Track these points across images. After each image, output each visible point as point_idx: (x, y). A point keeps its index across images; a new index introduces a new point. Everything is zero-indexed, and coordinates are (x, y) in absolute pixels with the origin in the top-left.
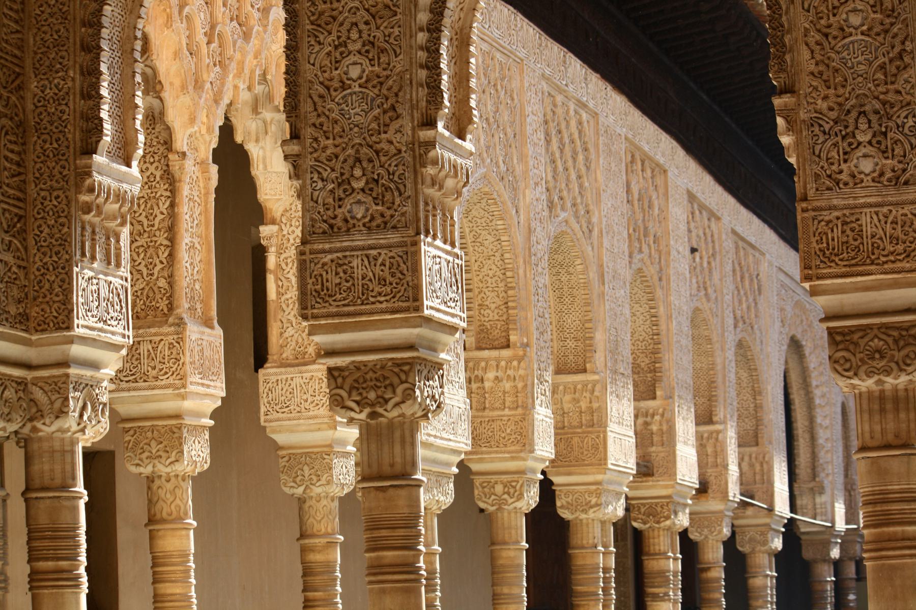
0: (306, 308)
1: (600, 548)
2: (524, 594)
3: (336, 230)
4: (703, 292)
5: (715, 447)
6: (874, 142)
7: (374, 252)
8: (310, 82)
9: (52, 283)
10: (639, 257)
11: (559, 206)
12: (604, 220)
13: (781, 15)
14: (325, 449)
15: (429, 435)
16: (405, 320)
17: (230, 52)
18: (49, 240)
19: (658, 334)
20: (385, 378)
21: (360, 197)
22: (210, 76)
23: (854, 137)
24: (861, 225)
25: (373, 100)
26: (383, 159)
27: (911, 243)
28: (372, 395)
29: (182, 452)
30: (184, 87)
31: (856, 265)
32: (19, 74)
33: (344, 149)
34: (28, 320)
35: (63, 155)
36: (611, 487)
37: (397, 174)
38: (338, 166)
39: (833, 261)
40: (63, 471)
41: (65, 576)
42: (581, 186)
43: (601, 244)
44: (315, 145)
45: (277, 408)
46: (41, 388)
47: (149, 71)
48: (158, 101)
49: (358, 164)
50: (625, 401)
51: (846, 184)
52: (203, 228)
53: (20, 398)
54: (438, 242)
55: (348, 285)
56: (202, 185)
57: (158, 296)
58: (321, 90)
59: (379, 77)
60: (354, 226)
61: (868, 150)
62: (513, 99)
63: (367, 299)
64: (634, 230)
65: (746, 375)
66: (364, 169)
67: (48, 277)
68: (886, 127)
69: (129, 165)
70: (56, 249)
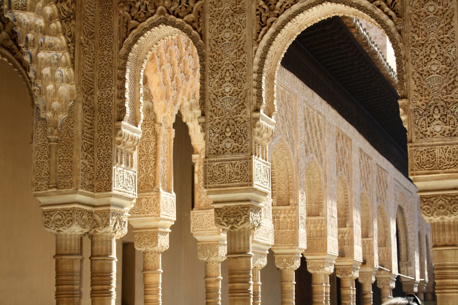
0: (206, 184)
1: (324, 285)
2: (294, 302)
3: (219, 153)
4: (365, 187)
5: (369, 246)
6: (441, 118)
7: (234, 162)
8: (210, 93)
9: (104, 173)
10: (341, 172)
11: (310, 152)
12: (327, 157)
13: (402, 67)
14: (216, 243)
15: (257, 238)
16: (246, 189)
17: (180, 85)
18: (103, 155)
19: (347, 202)
20: (238, 213)
21: (229, 139)
22: (172, 94)
23: (433, 116)
24: (435, 153)
25: (235, 101)
26: (238, 124)
27: (457, 160)
28: (232, 220)
29: (157, 242)
30: (161, 98)
32: (92, 88)
34: (94, 187)
35: (110, 121)
36: (328, 261)
37: (244, 131)
38: (221, 127)
40: (107, 249)
41: (106, 292)
42: (318, 144)
43: (326, 167)
44: (211, 119)
45: (197, 226)
46: (99, 215)
47: (147, 91)
48: (151, 103)
50: (334, 227)
51: (429, 136)
52: (168, 154)
53: (89, 219)
54: (260, 159)
55: (223, 175)
56: (168, 137)
57: (150, 180)
58: (214, 97)
59: (237, 91)
60: (226, 151)
61: (439, 122)
62: (292, 109)
64: (339, 162)
65: (381, 219)
66: (230, 129)
67: (102, 170)
68: (447, 113)
69: (137, 126)
70: (106, 159)
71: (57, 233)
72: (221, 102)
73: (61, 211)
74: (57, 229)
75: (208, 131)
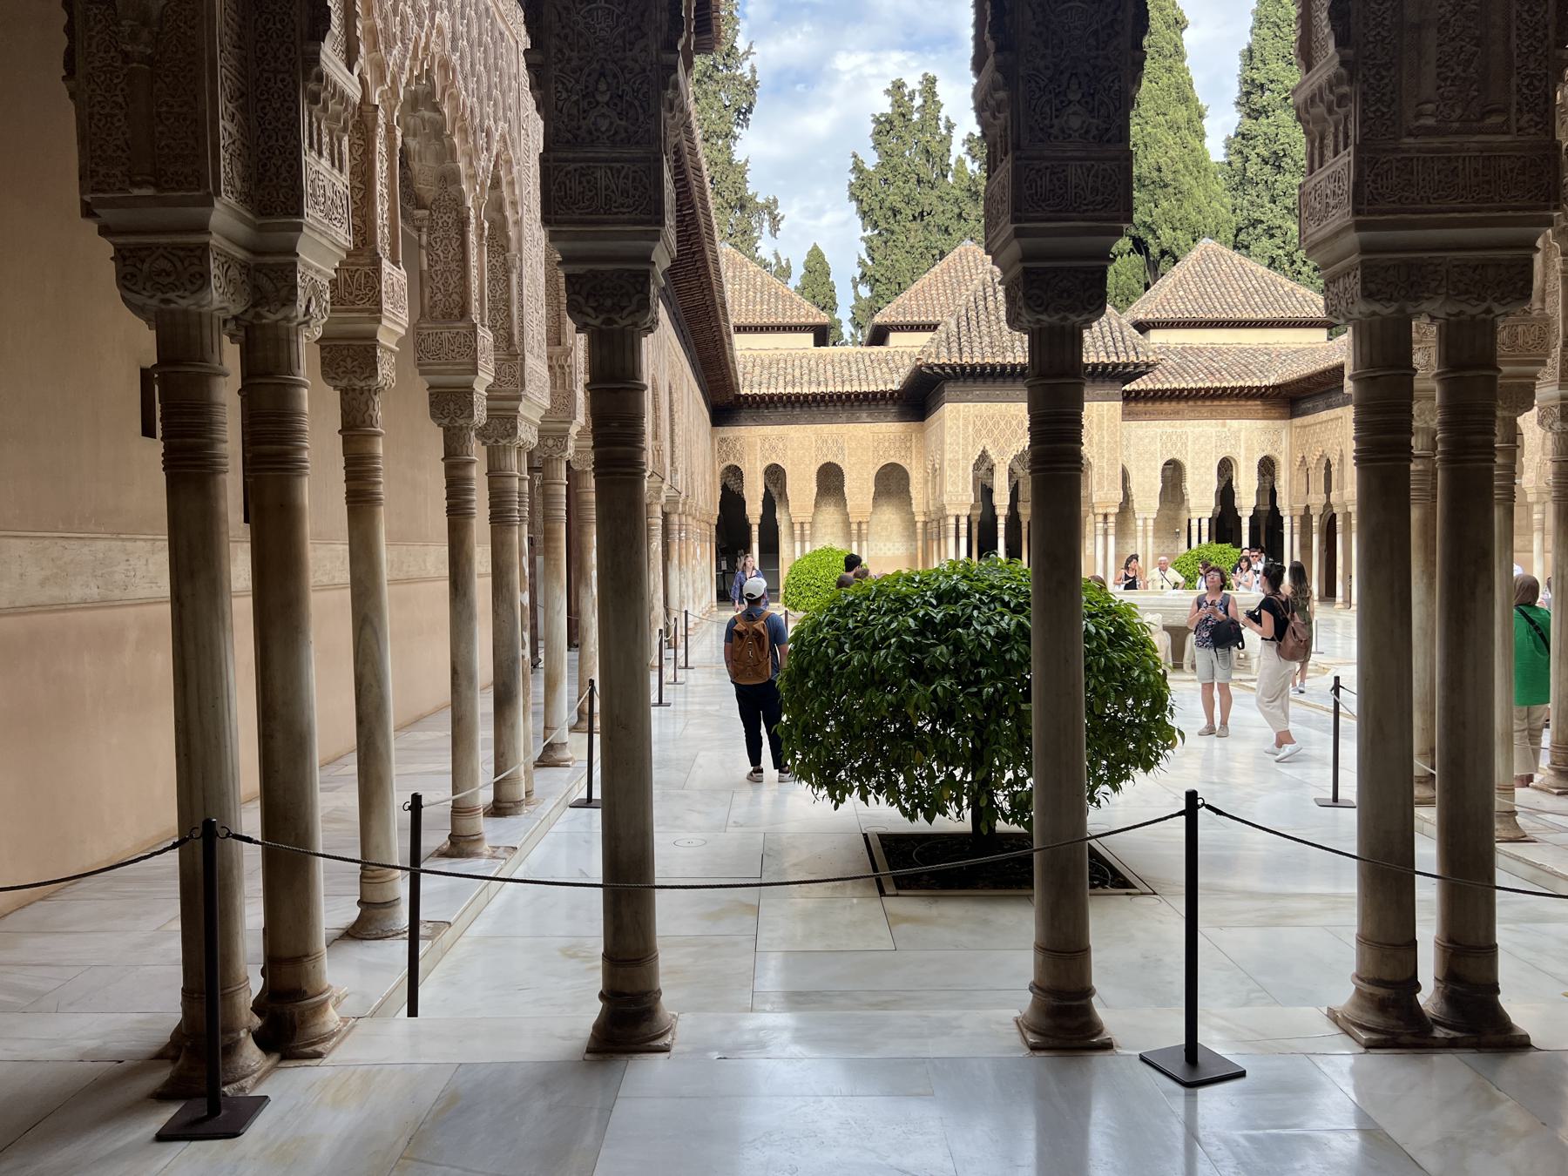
0: (550, 214)
3: (579, 140)
7: (618, 165)
20: (622, 287)
23: (1066, 96)
26: (628, 76)
28: (609, 303)
31: (1060, 211)
33: (589, 62)
37: (642, 91)
39: (1040, 206)
45: (429, 355)
46: (266, 275)
49: (602, 79)
53: (243, 282)
61: (1077, 108)
63: (610, 209)
67: (273, 161)
71: (163, 306)
72: (585, 18)
73: (169, 249)
74: (160, 295)
75: (553, 86)
